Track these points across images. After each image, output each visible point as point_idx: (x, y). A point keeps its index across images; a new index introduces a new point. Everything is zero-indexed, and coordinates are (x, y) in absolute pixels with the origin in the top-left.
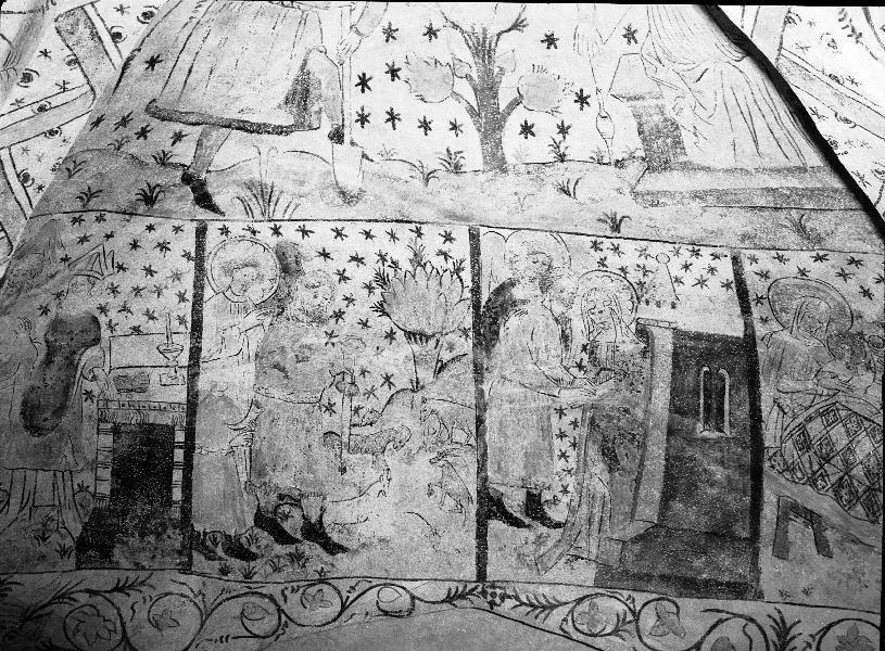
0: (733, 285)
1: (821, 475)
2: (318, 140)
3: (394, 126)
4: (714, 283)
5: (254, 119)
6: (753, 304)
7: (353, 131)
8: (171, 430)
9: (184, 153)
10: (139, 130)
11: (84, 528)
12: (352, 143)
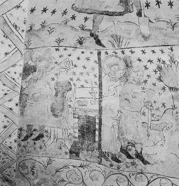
2: (132, 16)
3: (159, 6)
5: (111, 10)
7: (145, 11)
8: (94, 119)
9: (89, 25)
10: (63, 12)
11: (71, 147)
12: (145, 16)
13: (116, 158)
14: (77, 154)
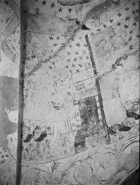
11: (76, 138)
13: (125, 127)
14: (83, 144)
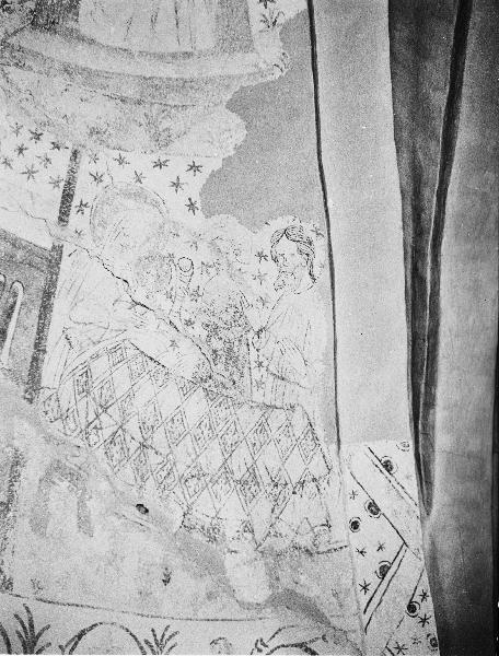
0: (62, 184)
1: (95, 428)
4: (44, 175)
6: (73, 210)
